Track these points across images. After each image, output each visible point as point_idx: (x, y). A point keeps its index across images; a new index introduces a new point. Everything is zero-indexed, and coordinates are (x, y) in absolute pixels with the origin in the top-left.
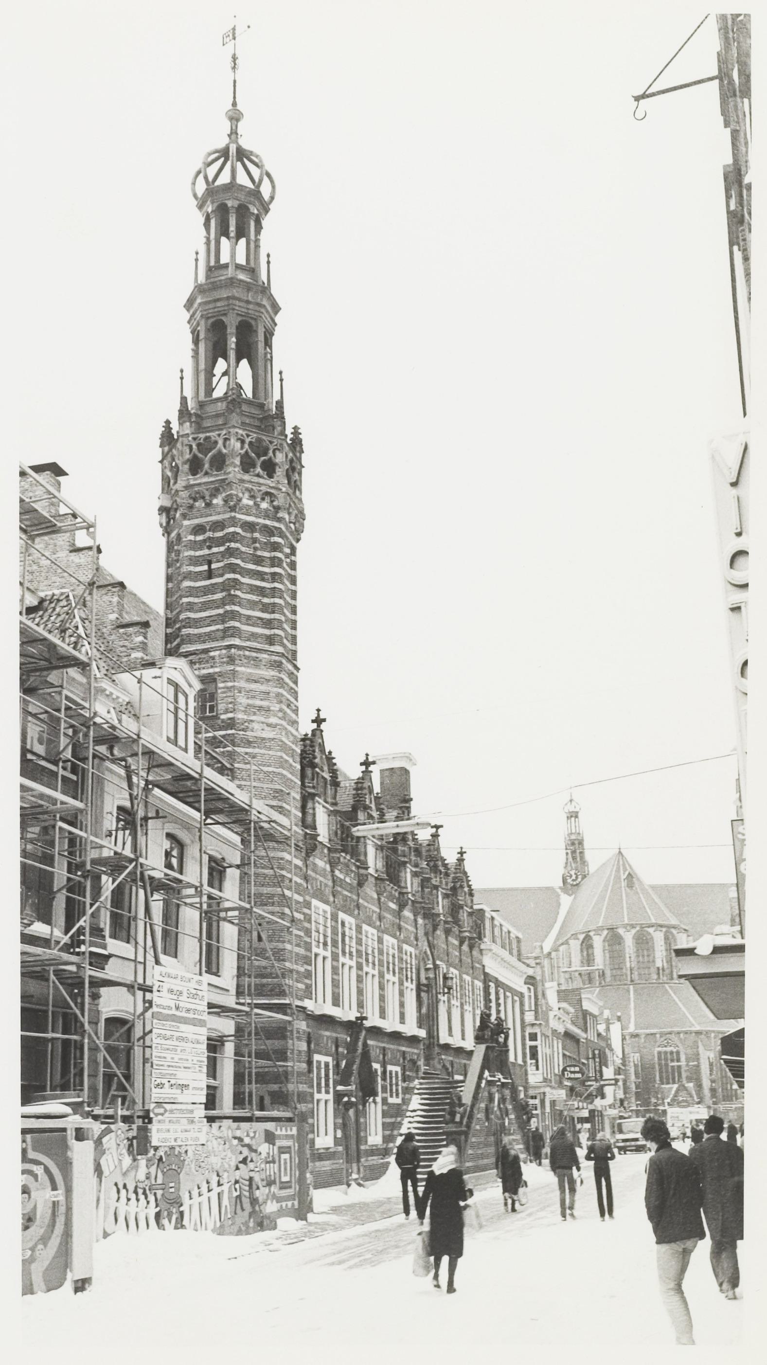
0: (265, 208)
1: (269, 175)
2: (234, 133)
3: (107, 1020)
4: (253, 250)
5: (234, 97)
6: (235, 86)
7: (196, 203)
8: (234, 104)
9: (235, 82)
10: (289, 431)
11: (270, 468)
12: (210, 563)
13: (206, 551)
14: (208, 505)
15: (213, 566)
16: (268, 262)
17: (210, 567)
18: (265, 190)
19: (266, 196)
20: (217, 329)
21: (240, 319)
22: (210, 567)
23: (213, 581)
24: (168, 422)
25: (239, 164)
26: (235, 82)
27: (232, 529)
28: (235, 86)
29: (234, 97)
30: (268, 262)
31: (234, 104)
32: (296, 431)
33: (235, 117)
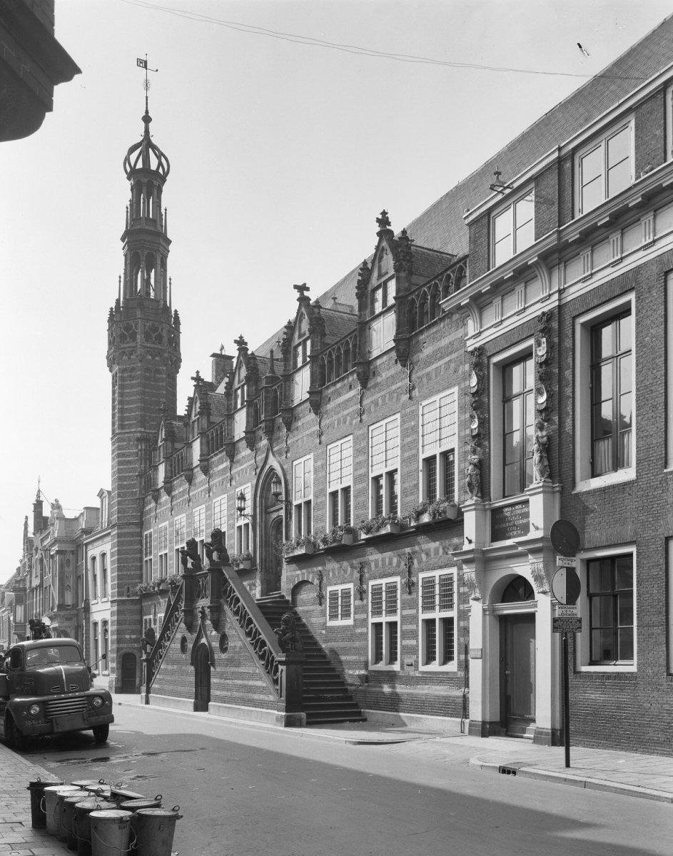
2: (147, 131)
4: (158, 205)
5: (147, 108)
6: (147, 100)
7: (126, 176)
8: (147, 112)
9: (147, 97)
10: (173, 313)
11: (160, 338)
14: (129, 358)
24: (112, 309)
25: (150, 150)
26: (147, 97)
28: (147, 100)
29: (147, 108)
31: (147, 112)
32: (176, 311)
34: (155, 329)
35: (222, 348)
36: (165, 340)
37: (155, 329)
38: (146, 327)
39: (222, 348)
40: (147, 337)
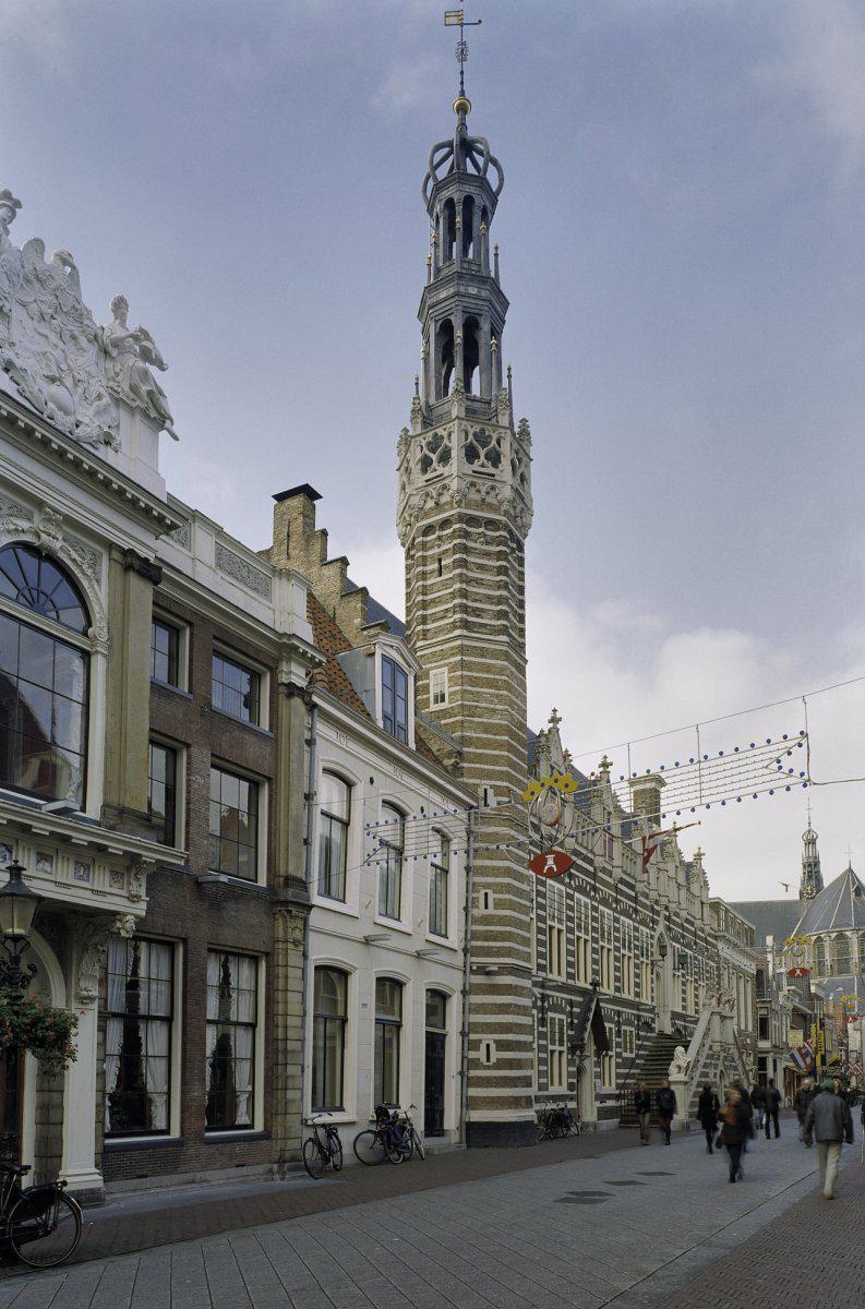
0: (493, 198)
1: (495, 162)
2: (463, 124)
3: (317, 968)
8: (462, 93)
12: (440, 560)
13: (436, 550)
15: (443, 563)
16: (496, 255)
17: (440, 563)
18: (492, 176)
19: (494, 182)
20: (446, 328)
21: (467, 315)
22: (440, 563)
23: (444, 577)
27: (457, 526)
30: (496, 255)
31: (462, 93)
32: (524, 421)
33: (463, 109)
34: (482, 438)
35: (648, 771)
36: (505, 463)
37: (482, 438)
38: (471, 437)
39: (648, 771)
40: (471, 454)
